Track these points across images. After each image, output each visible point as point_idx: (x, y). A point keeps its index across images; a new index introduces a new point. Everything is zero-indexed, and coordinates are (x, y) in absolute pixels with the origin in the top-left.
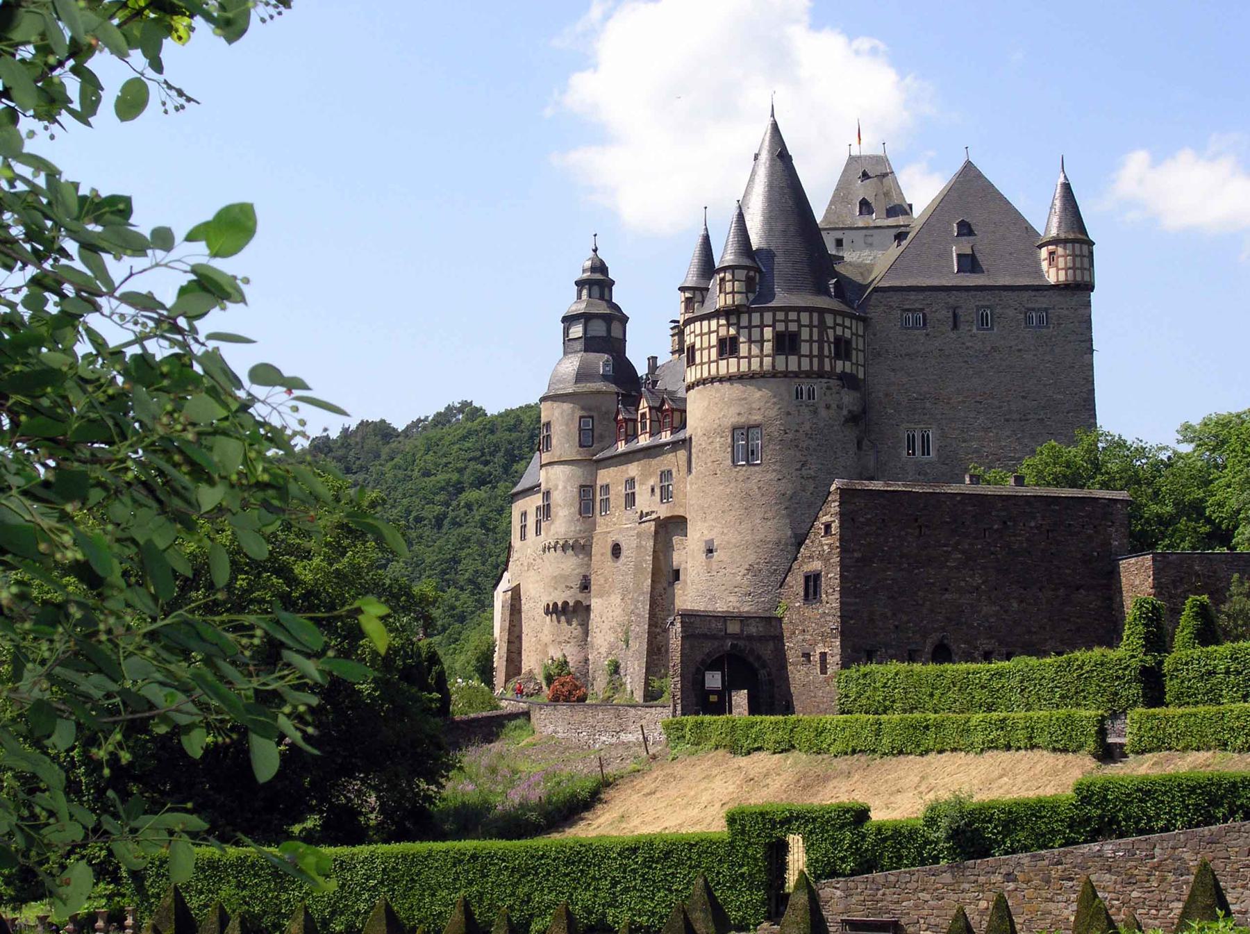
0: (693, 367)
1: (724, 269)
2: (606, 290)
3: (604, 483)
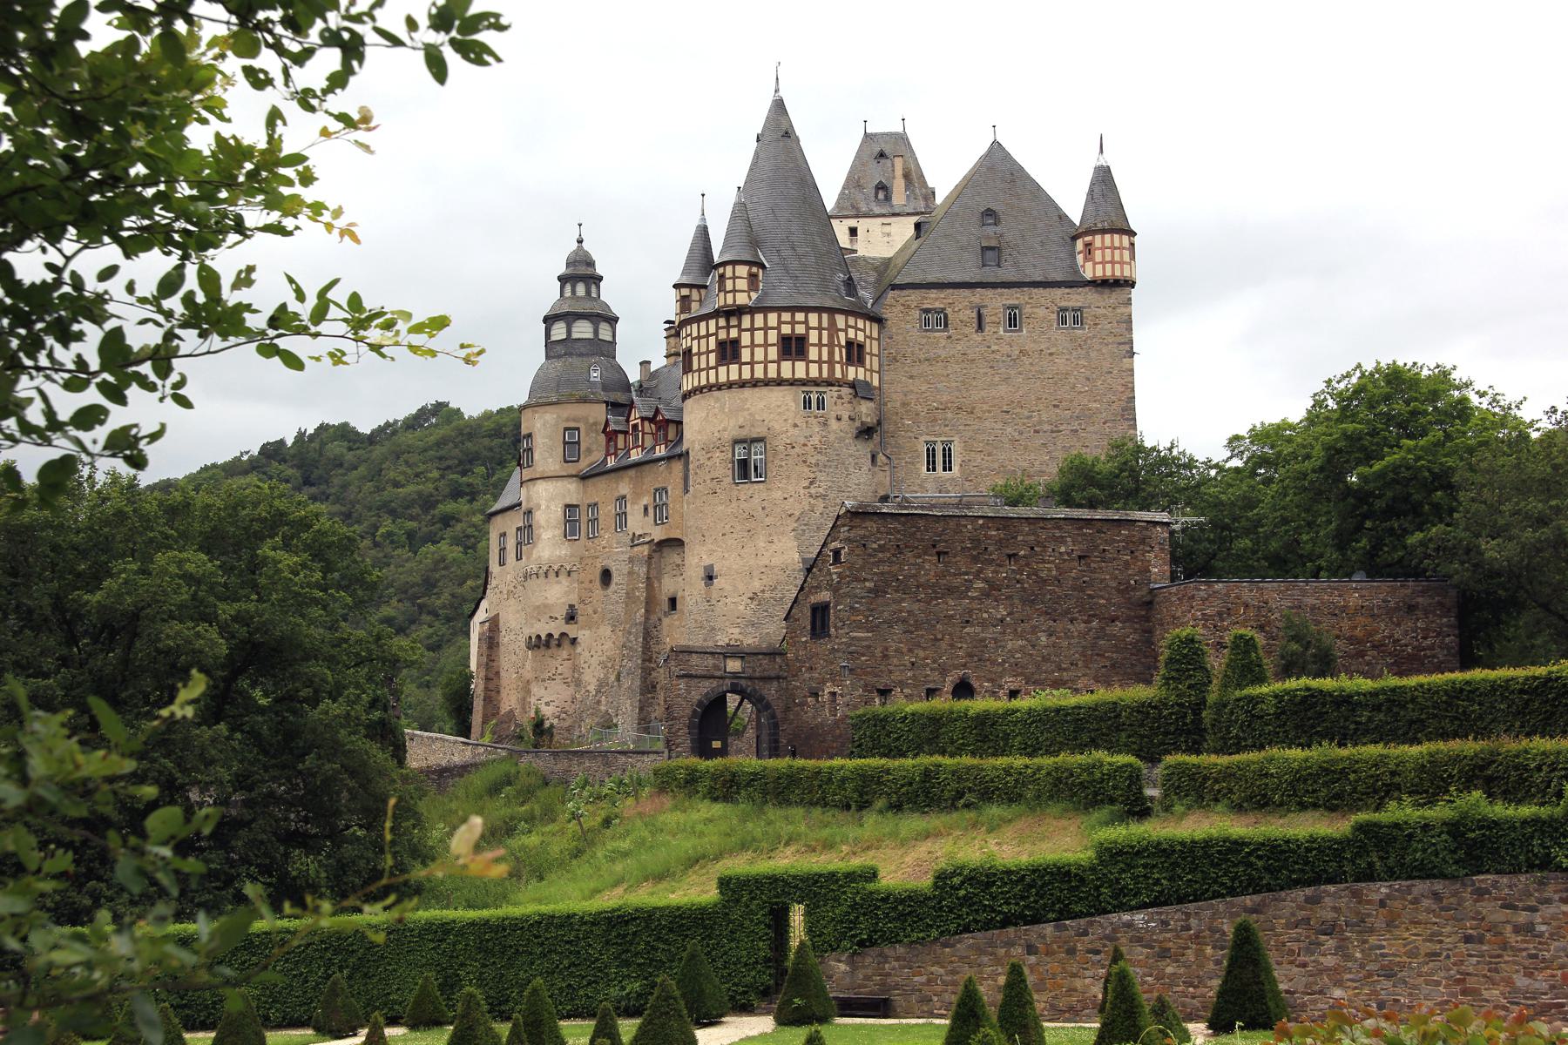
0: (690, 375)
1: (724, 264)
2: (593, 287)
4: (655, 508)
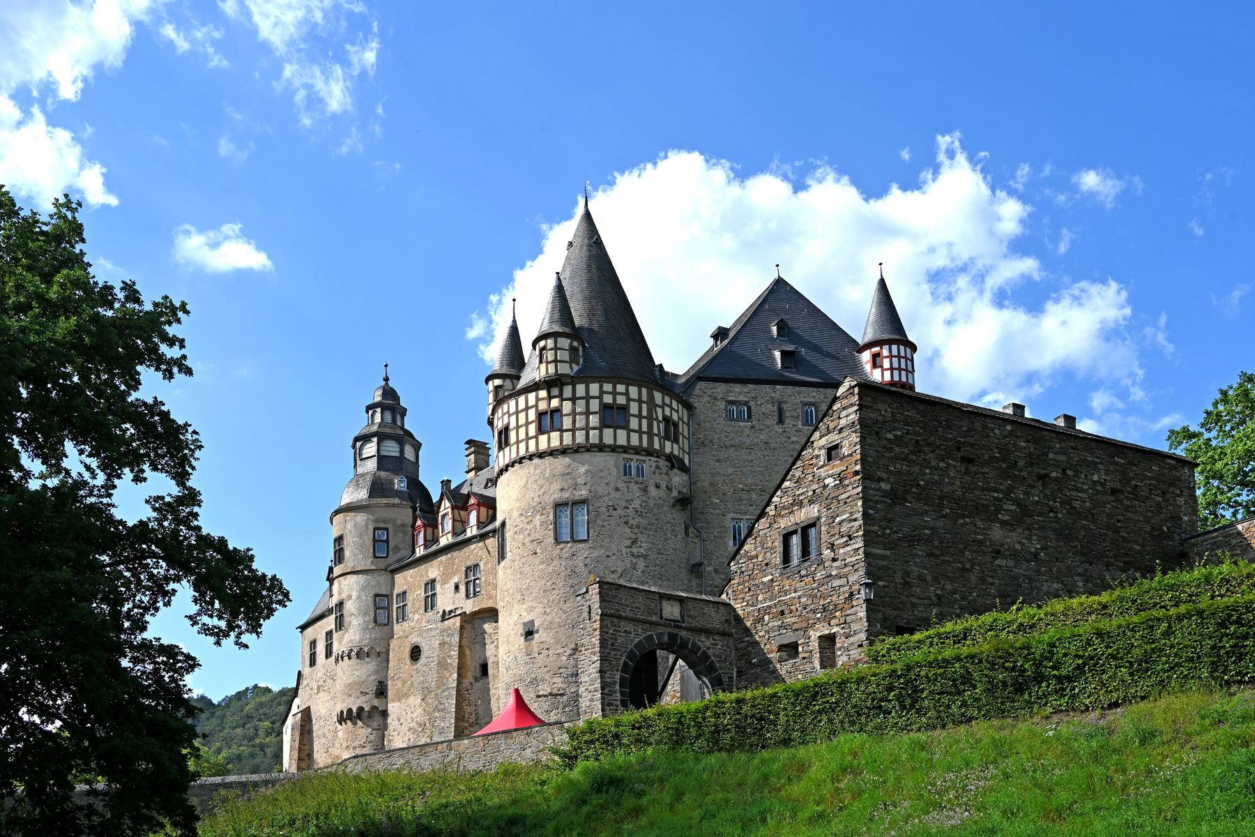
0: (507, 450)
3: (401, 590)
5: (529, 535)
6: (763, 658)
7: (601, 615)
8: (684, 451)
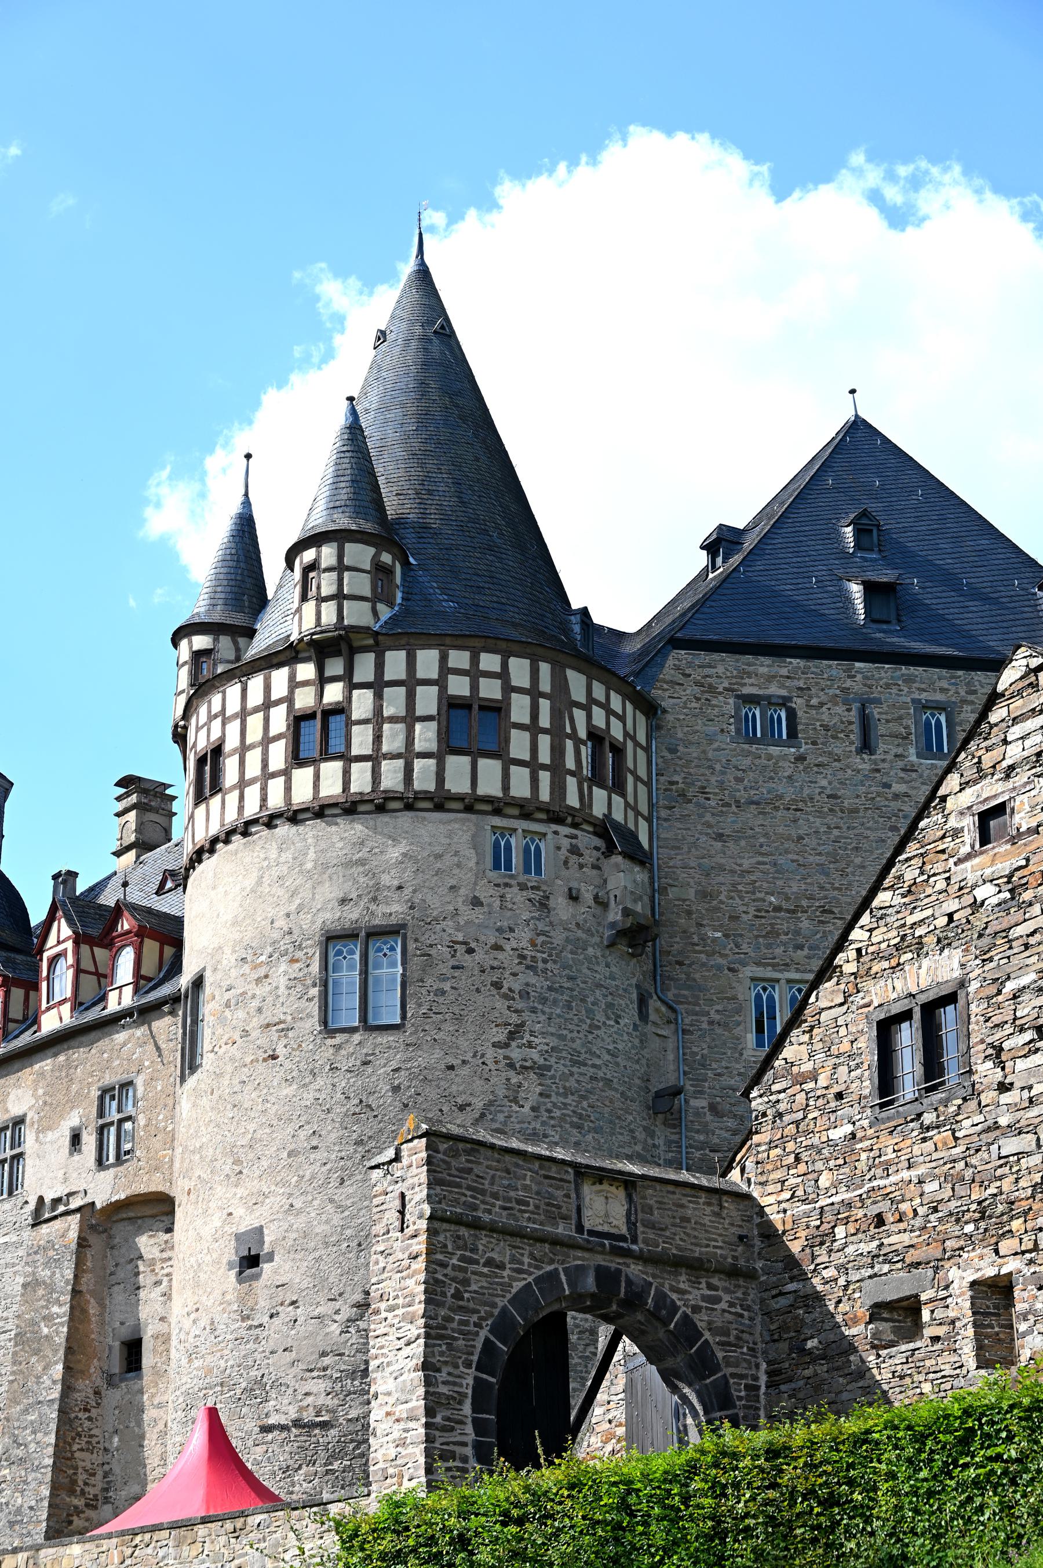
0: (215, 802)
4: (101, 1130)
5: (260, 1010)
6: (832, 1337)
7: (431, 1218)
8: (638, 813)
